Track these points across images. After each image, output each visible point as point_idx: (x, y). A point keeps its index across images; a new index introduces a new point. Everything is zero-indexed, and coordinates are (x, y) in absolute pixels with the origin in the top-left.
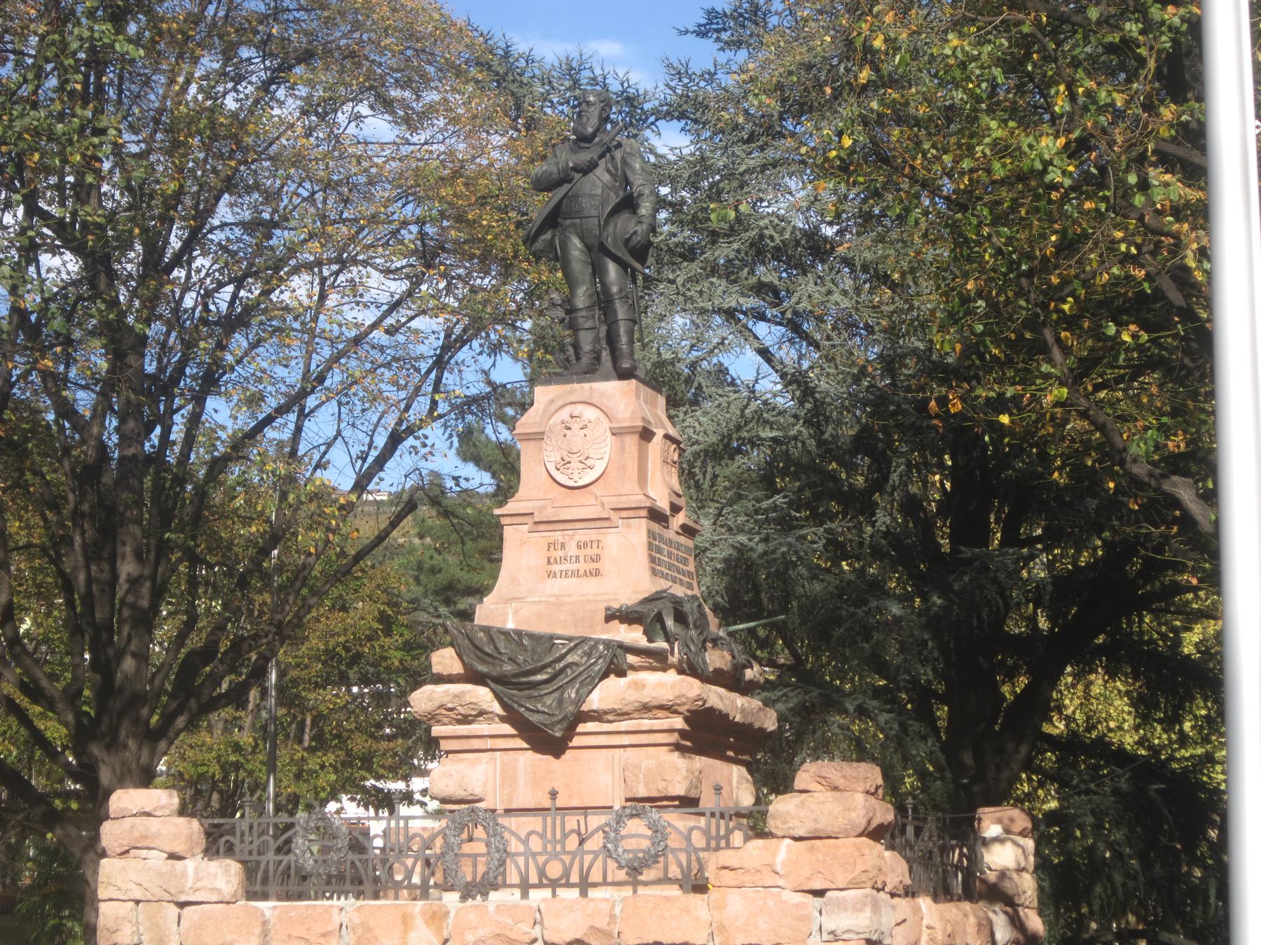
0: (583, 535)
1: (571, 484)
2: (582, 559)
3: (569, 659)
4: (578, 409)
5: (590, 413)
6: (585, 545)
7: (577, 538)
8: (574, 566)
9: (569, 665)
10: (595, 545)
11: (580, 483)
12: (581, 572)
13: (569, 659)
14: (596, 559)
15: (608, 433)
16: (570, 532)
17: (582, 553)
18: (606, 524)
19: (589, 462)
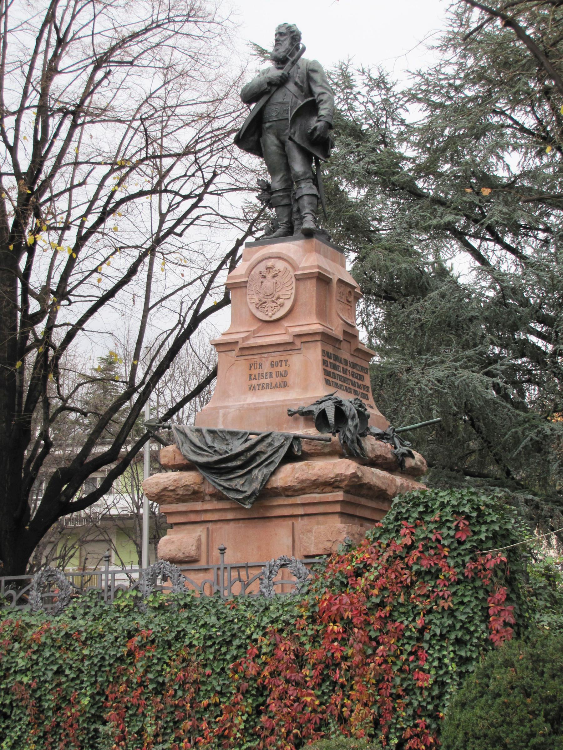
0: (276, 357)
1: (268, 319)
2: (274, 376)
3: (258, 449)
4: (270, 263)
5: (280, 265)
6: (277, 364)
7: (271, 359)
8: (268, 381)
9: (258, 454)
10: (284, 364)
11: (274, 318)
12: (273, 385)
13: (258, 449)
14: (284, 375)
15: (293, 279)
16: (266, 355)
17: (274, 370)
18: (289, 347)
19: (280, 301)
